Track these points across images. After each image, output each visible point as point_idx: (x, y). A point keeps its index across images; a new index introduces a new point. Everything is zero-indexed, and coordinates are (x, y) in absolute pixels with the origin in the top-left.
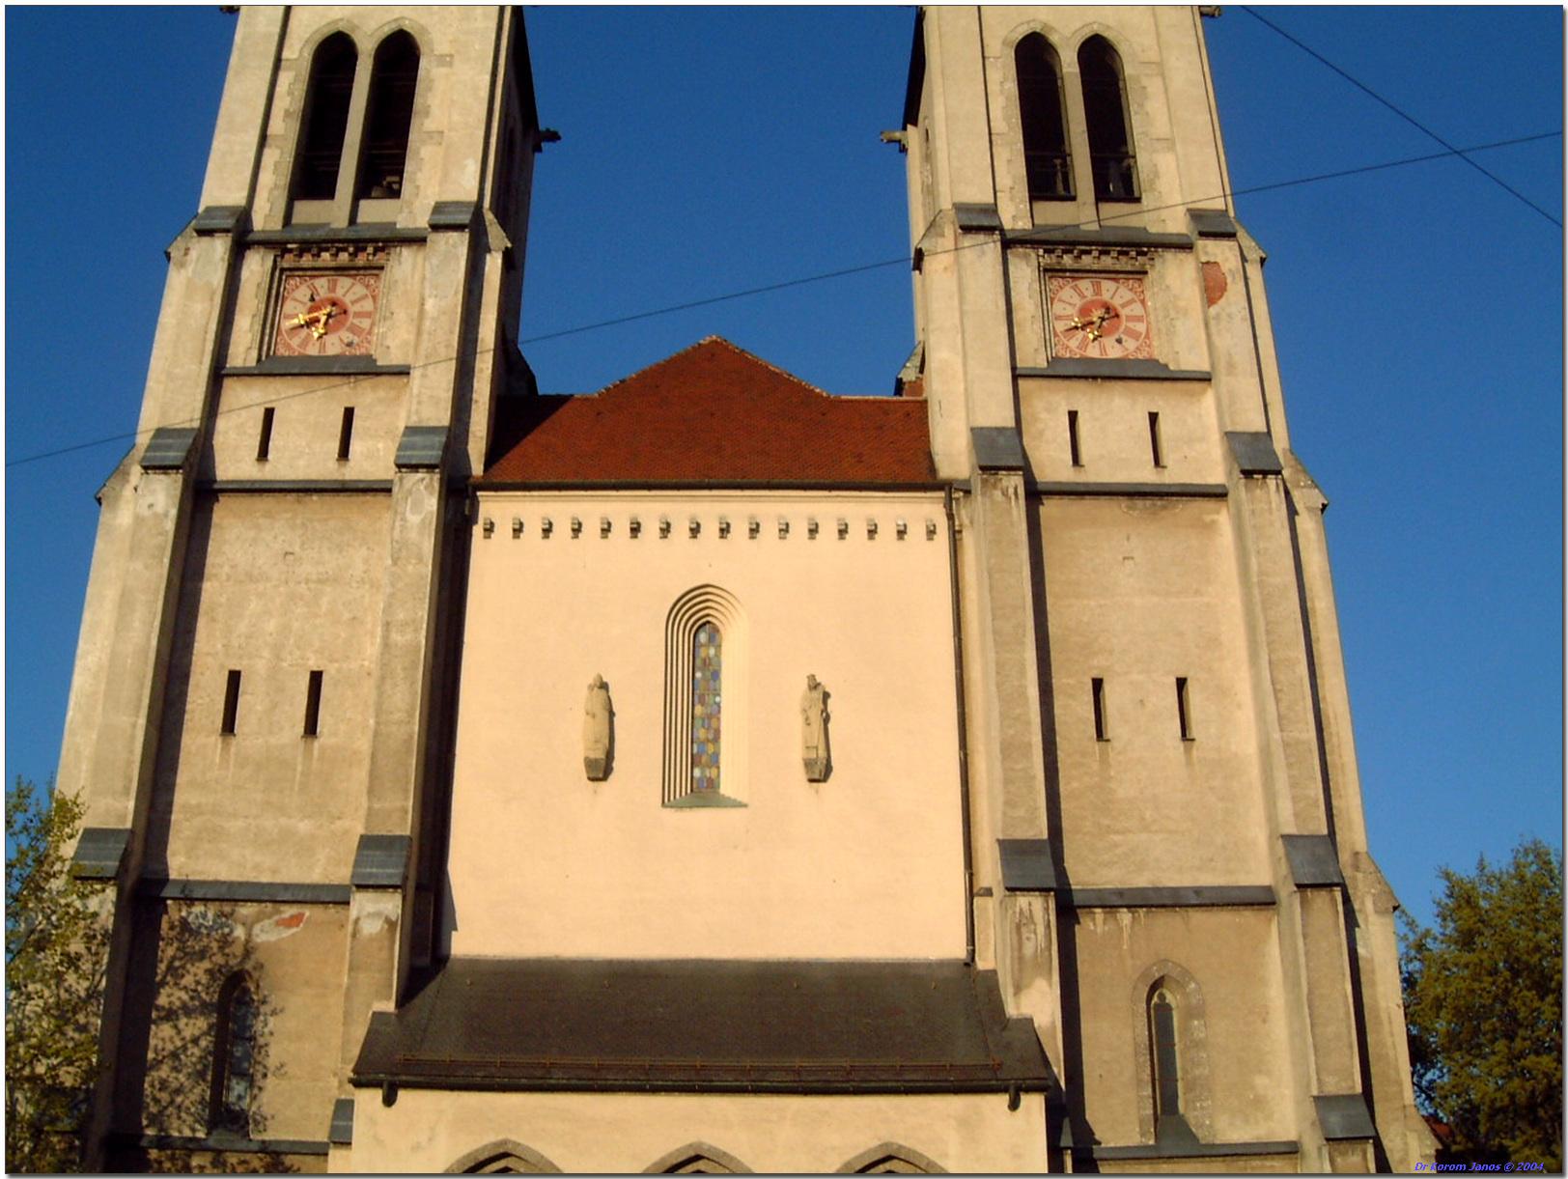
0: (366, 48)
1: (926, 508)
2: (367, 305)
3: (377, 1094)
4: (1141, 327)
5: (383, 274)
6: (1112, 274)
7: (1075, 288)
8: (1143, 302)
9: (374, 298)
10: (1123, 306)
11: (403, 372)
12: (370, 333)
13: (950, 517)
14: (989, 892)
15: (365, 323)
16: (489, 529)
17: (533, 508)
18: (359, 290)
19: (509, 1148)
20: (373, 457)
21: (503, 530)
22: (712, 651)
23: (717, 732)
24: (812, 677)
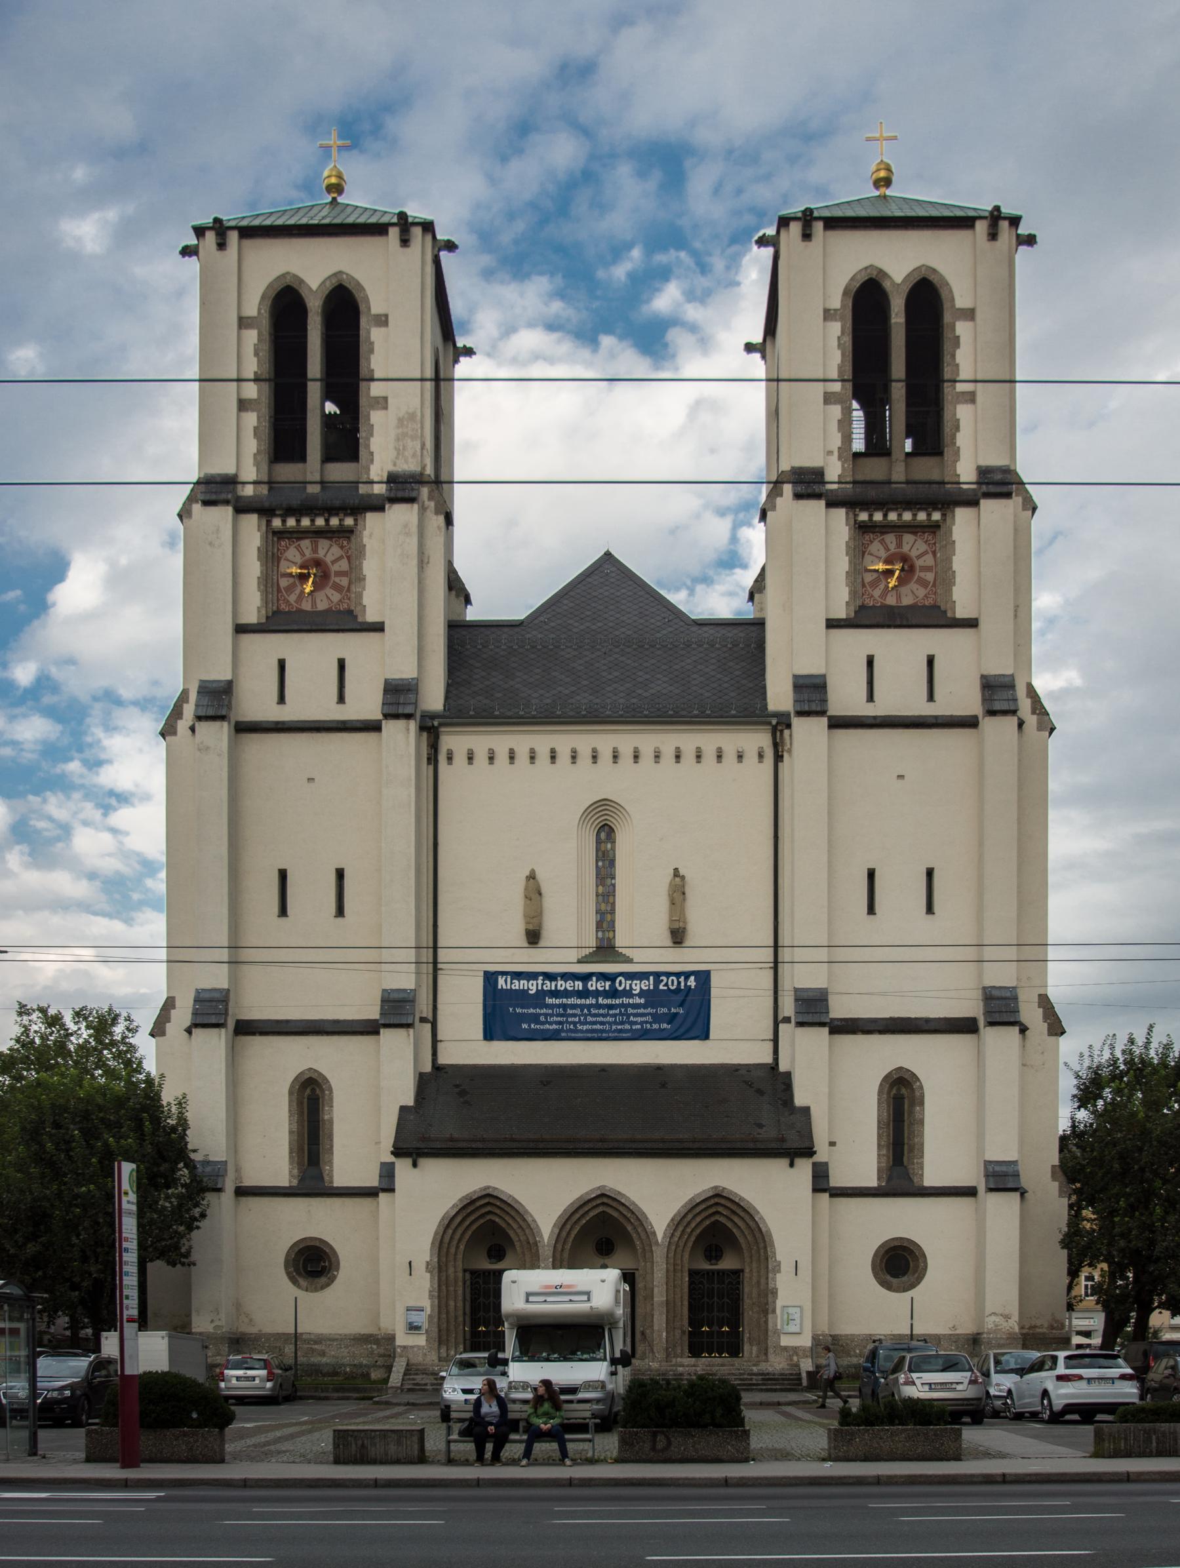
0: (314, 305)
1: (757, 740)
2: (343, 565)
3: (409, 1161)
4: (929, 577)
5: (353, 538)
6: (914, 528)
7: (882, 542)
8: (934, 553)
9: (349, 558)
10: (918, 557)
11: (379, 628)
12: (349, 590)
13: (776, 745)
14: (787, 1020)
15: (344, 582)
16: (450, 759)
17: (480, 741)
18: (336, 551)
19: (490, 1191)
20: (365, 702)
21: (460, 758)
22: (609, 846)
23: (613, 904)
24: (676, 870)
